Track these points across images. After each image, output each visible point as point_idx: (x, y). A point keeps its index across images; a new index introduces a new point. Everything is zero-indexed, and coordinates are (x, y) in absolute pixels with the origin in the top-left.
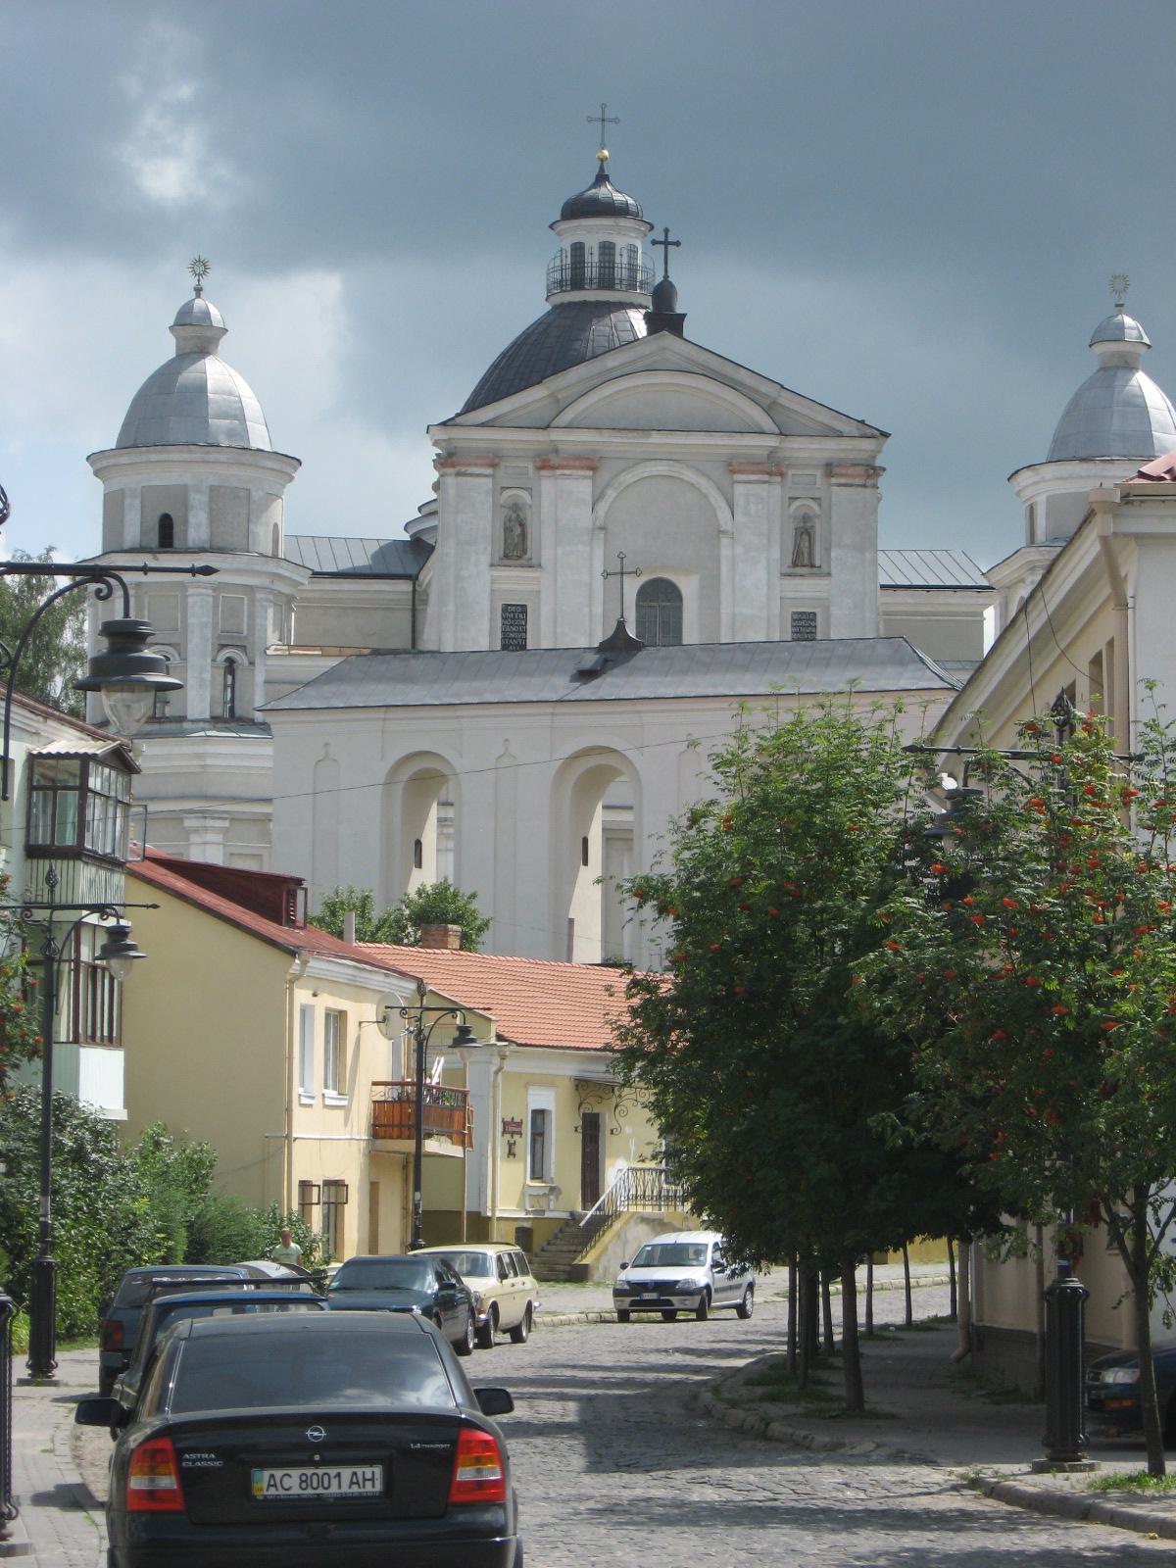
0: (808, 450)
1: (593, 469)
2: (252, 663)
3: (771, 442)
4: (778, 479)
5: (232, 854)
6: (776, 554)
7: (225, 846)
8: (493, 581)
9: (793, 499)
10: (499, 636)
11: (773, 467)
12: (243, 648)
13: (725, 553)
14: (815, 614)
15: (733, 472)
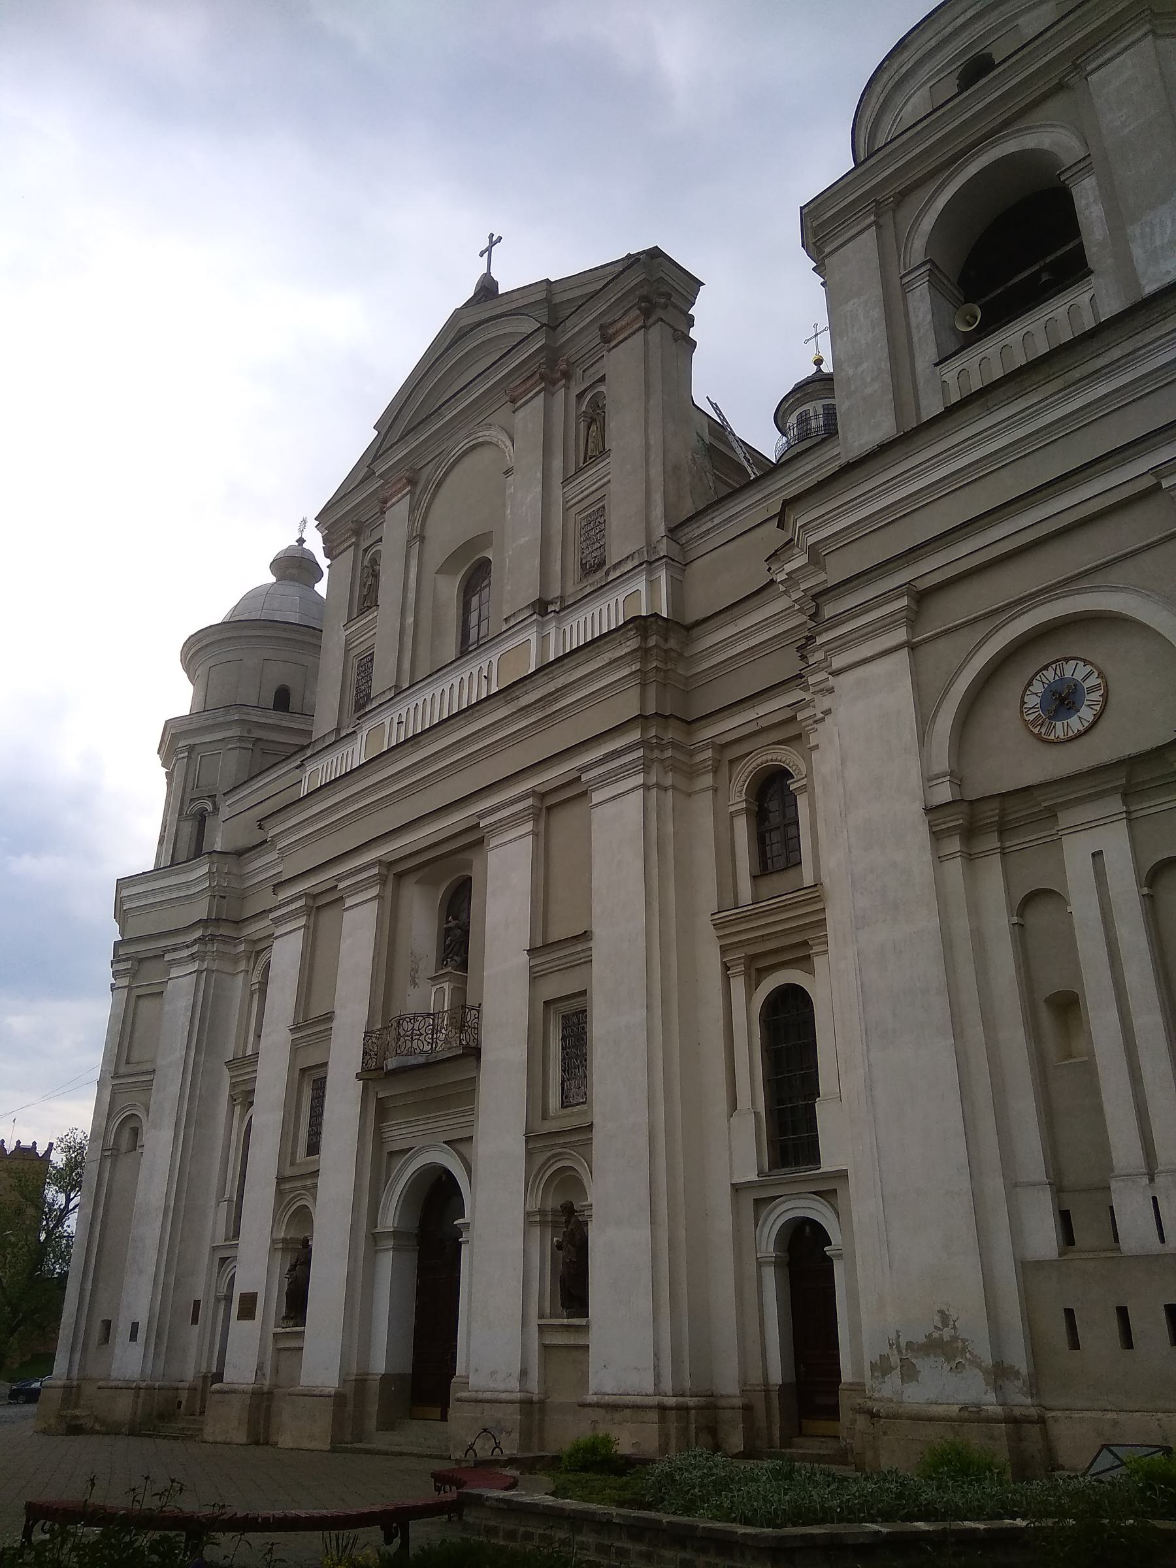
0: (579, 330)
1: (412, 482)
2: (216, 809)
3: (538, 343)
4: (563, 381)
5: (139, 997)
6: (558, 463)
7: (130, 988)
8: (348, 642)
9: (580, 396)
10: (351, 693)
11: (551, 371)
12: (212, 797)
13: (508, 492)
14: (603, 507)
15: (513, 401)
